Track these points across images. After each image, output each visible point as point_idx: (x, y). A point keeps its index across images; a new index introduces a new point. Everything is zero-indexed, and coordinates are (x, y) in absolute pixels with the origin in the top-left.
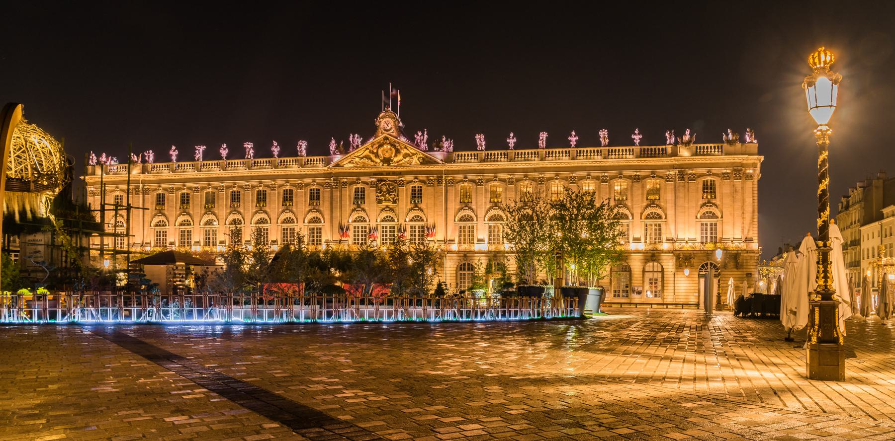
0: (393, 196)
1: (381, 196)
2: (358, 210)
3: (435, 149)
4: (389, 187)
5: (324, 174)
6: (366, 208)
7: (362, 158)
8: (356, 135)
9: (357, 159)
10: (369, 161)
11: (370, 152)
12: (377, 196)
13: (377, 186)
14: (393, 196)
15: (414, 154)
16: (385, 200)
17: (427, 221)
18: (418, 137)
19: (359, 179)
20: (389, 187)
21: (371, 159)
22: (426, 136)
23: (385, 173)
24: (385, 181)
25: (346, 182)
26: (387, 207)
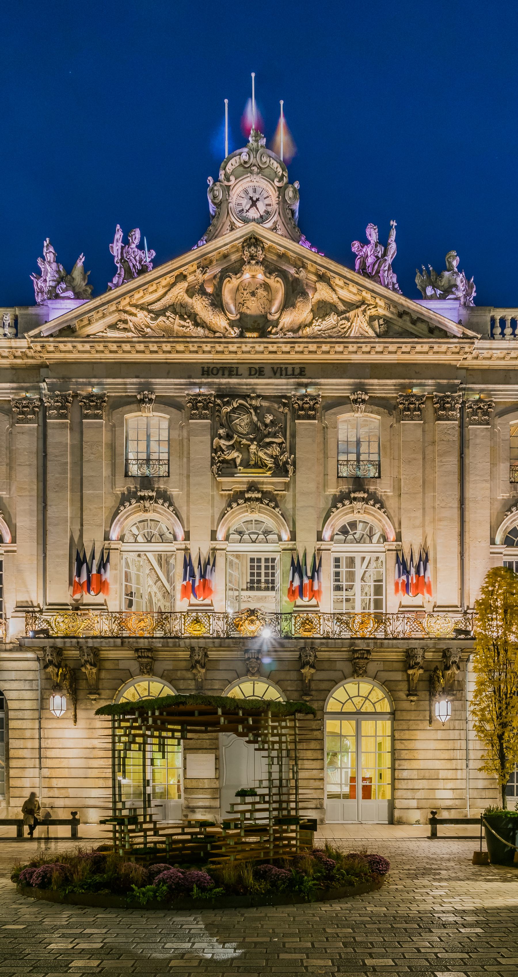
0: (275, 450)
1: (232, 447)
2: (143, 498)
3: (429, 291)
4: (261, 418)
5: (14, 368)
6: (174, 492)
7: (158, 314)
8: (137, 234)
9: (142, 317)
10: (189, 323)
11: (190, 292)
12: (216, 450)
13: (215, 412)
14: (275, 450)
15: (351, 306)
16: (246, 464)
17: (399, 538)
18: (368, 250)
19: (149, 387)
20: (261, 418)
21: (193, 317)
22: (393, 247)
23: (243, 370)
24: (245, 397)
25: (101, 397)
26: (253, 487)
